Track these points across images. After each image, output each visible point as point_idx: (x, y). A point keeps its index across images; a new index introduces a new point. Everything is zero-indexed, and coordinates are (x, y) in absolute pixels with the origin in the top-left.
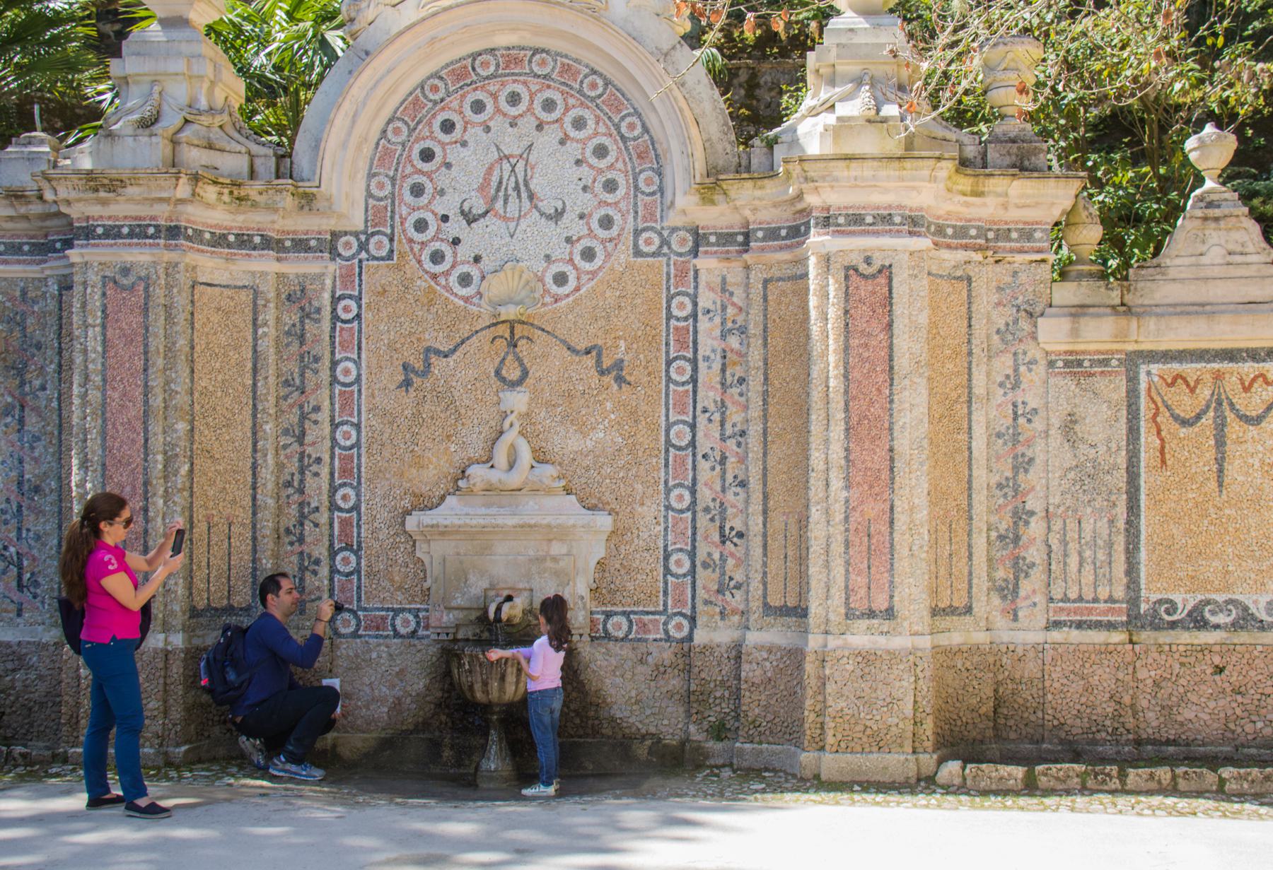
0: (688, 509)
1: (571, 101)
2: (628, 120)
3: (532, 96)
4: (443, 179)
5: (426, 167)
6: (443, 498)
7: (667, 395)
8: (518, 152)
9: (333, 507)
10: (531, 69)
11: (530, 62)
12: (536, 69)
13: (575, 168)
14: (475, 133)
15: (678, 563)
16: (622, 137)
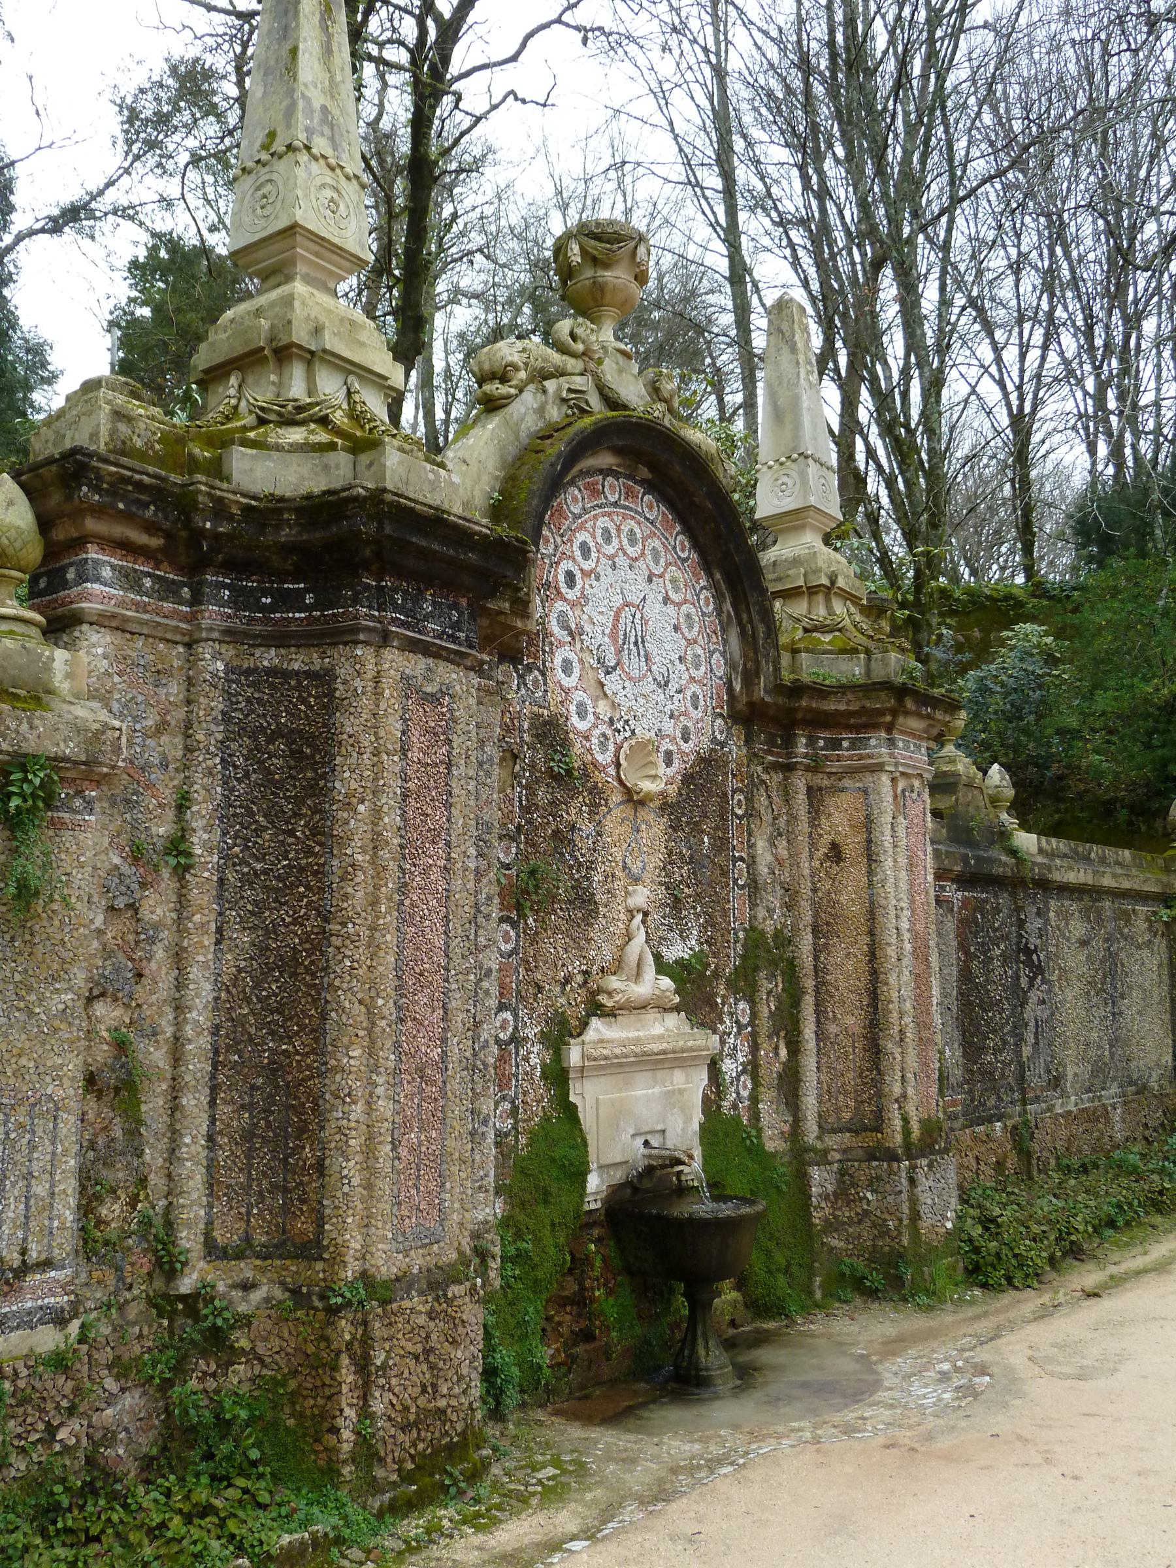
14: (604, 568)
15: (745, 1087)
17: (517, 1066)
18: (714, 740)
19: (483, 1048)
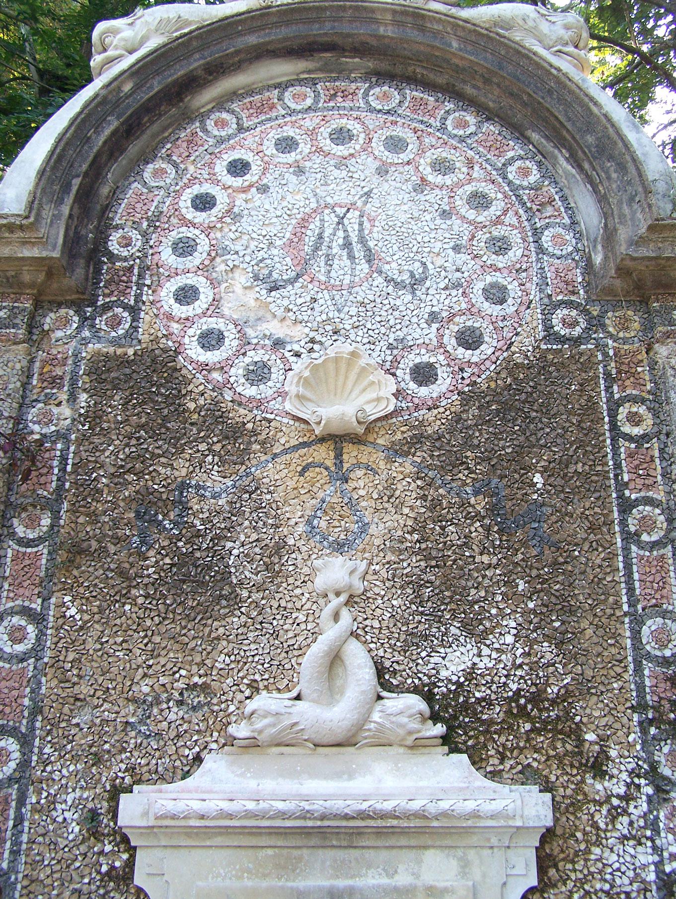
4: (226, 235)
5: (200, 217)
7: (628, 566)
10: (367, 102)
11: (366, 94)
13: (438, 221)
16: (510, 183)
18: (550, 335)
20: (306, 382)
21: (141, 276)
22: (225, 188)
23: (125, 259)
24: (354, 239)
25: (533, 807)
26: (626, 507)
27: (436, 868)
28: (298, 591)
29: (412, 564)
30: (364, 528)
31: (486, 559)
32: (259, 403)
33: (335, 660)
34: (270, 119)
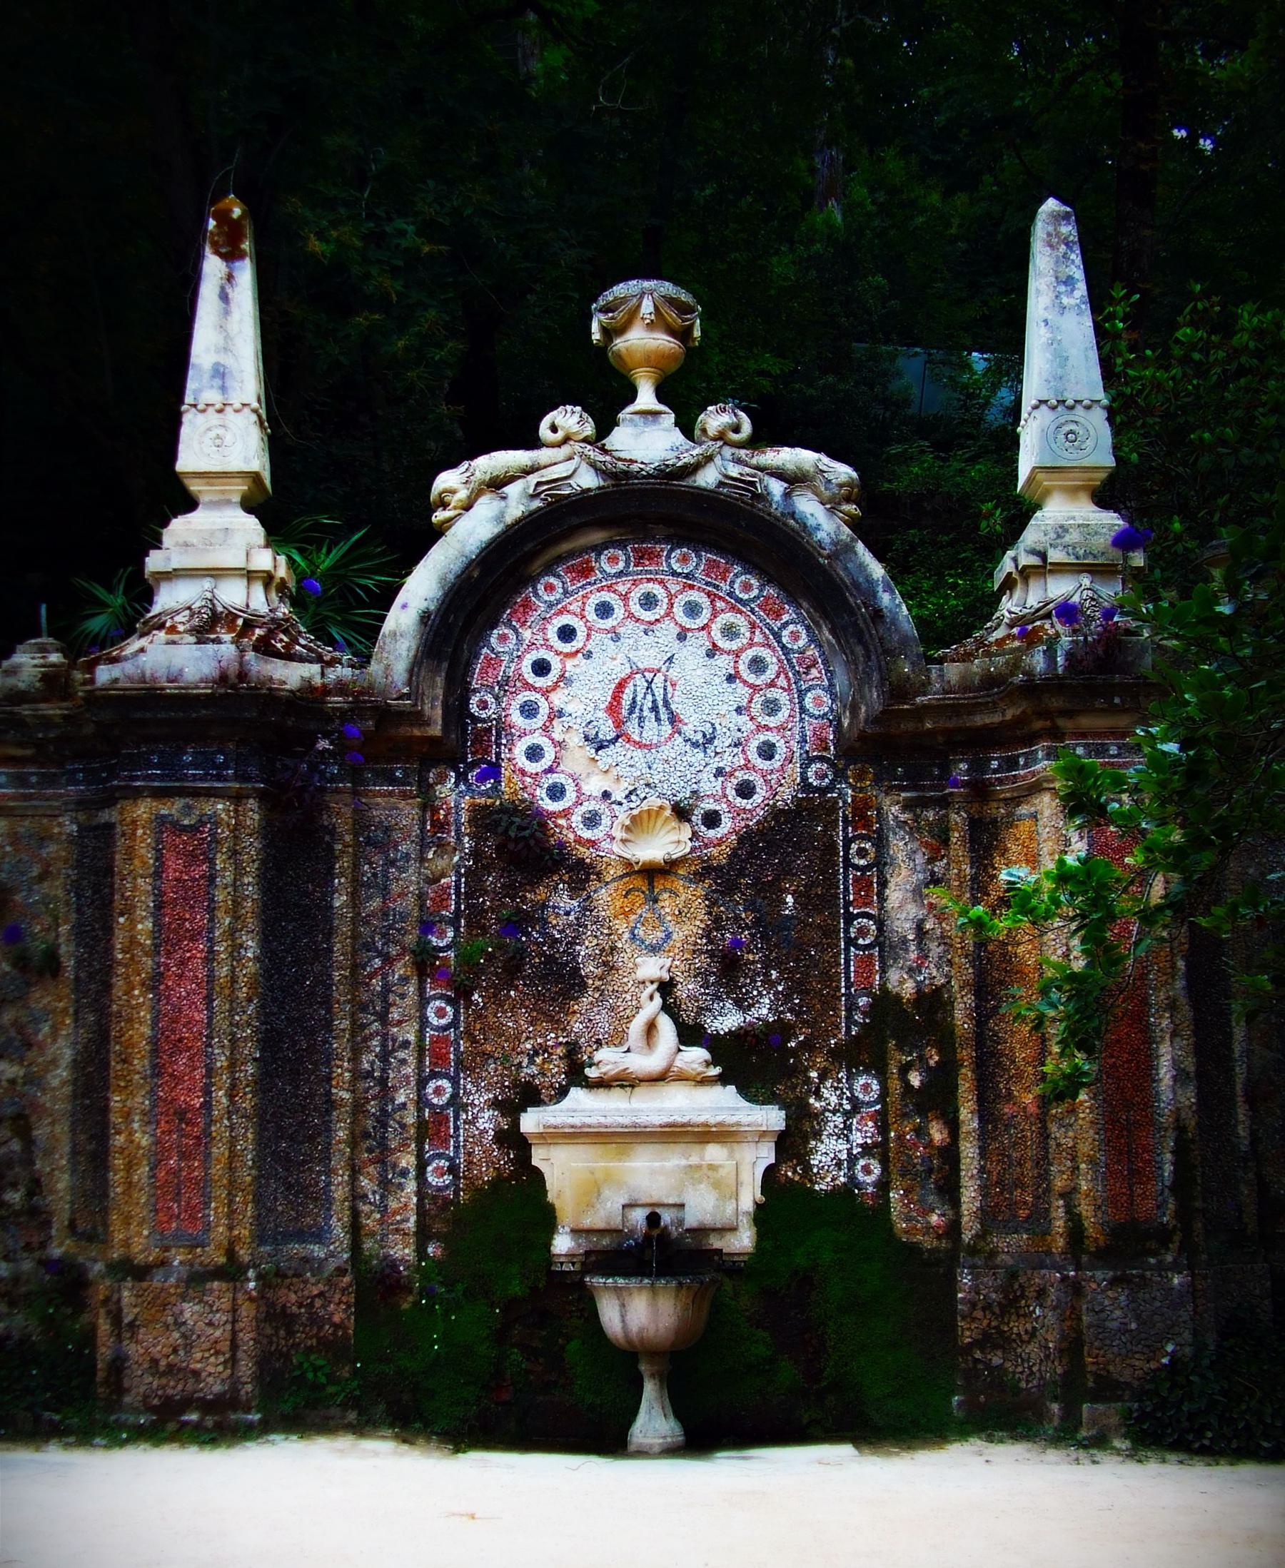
0: (876, 1102)
1: (720, 604)
2: (791, 628)
3: (671, 597)
5: (541, 682)
6: (562, 1093)
8: (656, 664)
9: (422, 1102)
10: (669, 565)
11: (668, 557)
12: (676, 566)
13: (725, 685)
17: (457, 1128)
18: (805, 785)
19: (400, 1109)
20: (628, 829)
21: (499, 736)
22: (558, 653)
23: (484, 721)
24: (660, 703)
25: (773, 1118)
26: (850, 919)
27: (714, 1153)
28: (625, 980)
29: (702, 961)
30: (669, 936)
31: (751, 957)
32: (592, 843)
33: (651, 1028)
34: (589, 583)
